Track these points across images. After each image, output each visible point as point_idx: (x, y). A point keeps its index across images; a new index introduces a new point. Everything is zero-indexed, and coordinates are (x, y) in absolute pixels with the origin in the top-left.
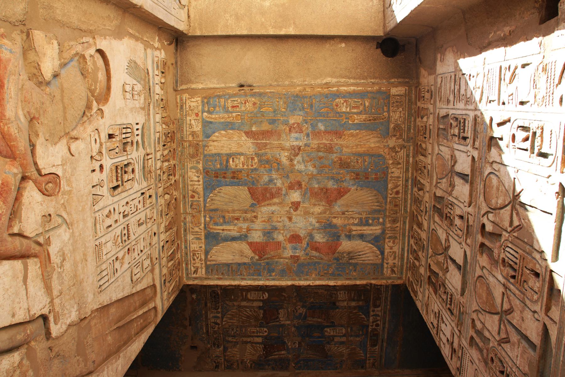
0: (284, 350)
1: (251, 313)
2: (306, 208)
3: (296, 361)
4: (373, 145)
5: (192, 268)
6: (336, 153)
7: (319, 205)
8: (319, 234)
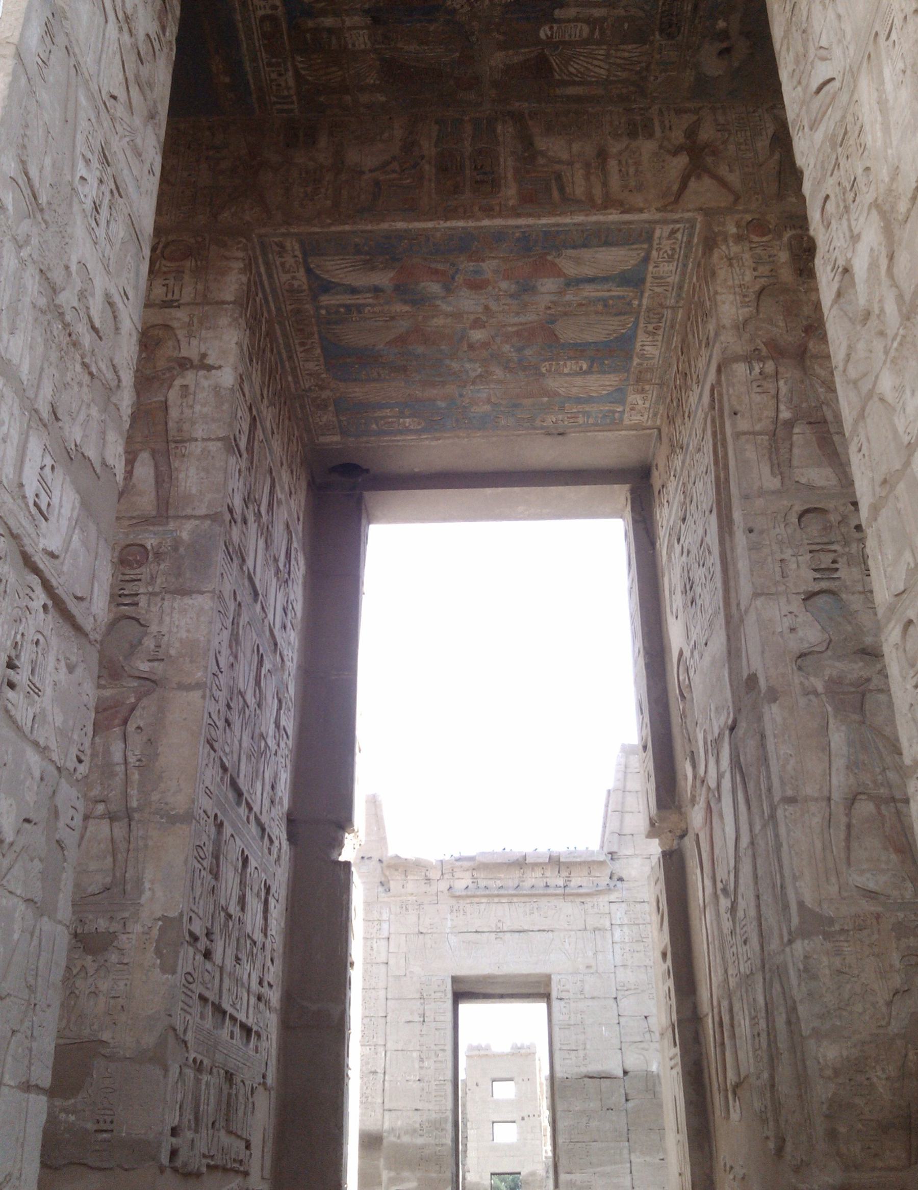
4: (357, 390)
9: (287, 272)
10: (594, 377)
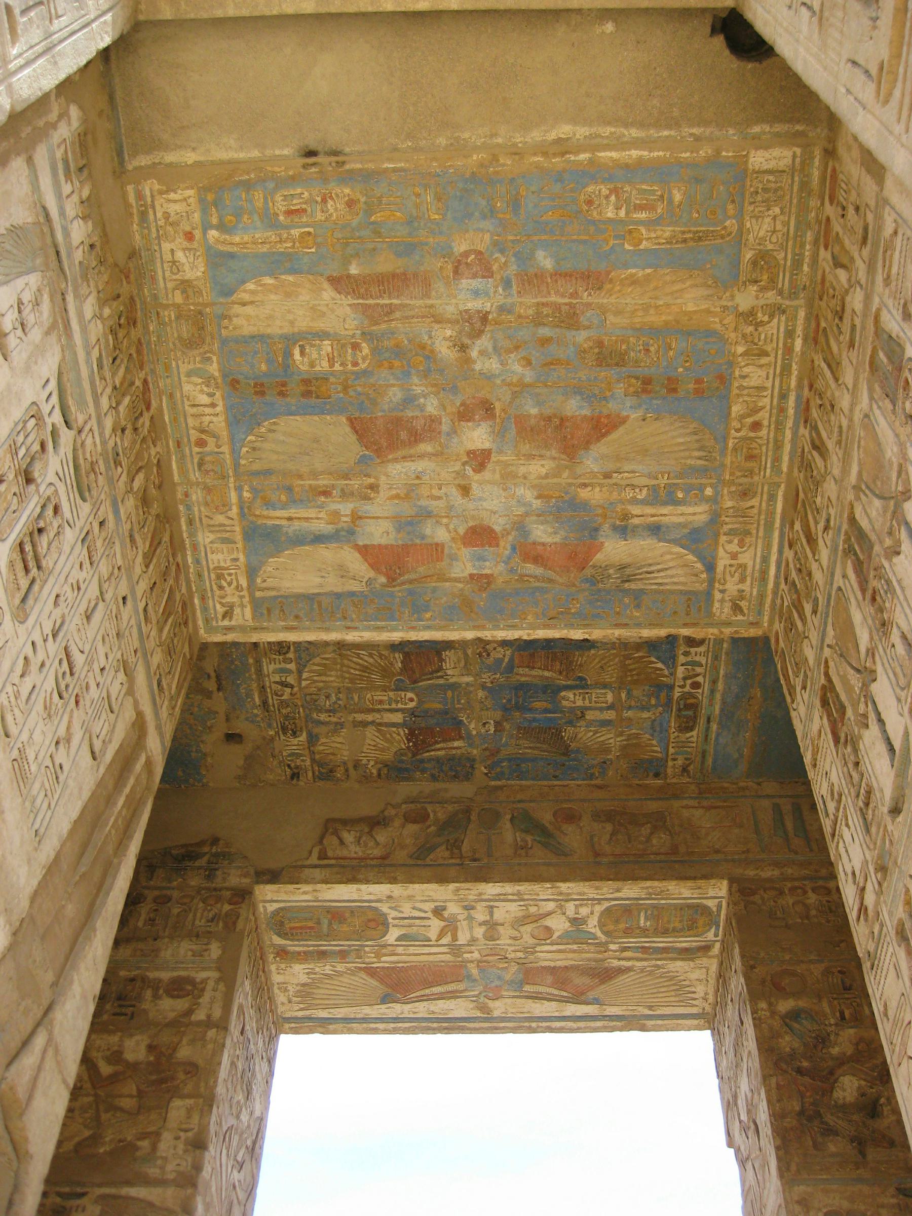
0: (461, 738)
1: (371, 660)
2: (506, 465)
3: (489, 762)
4: (691, 307)
5: (218, 606)
6: (588, 328)
7: (541, 456)
8: (542, 524)
9: (740, 566)
10: (278, 328)
